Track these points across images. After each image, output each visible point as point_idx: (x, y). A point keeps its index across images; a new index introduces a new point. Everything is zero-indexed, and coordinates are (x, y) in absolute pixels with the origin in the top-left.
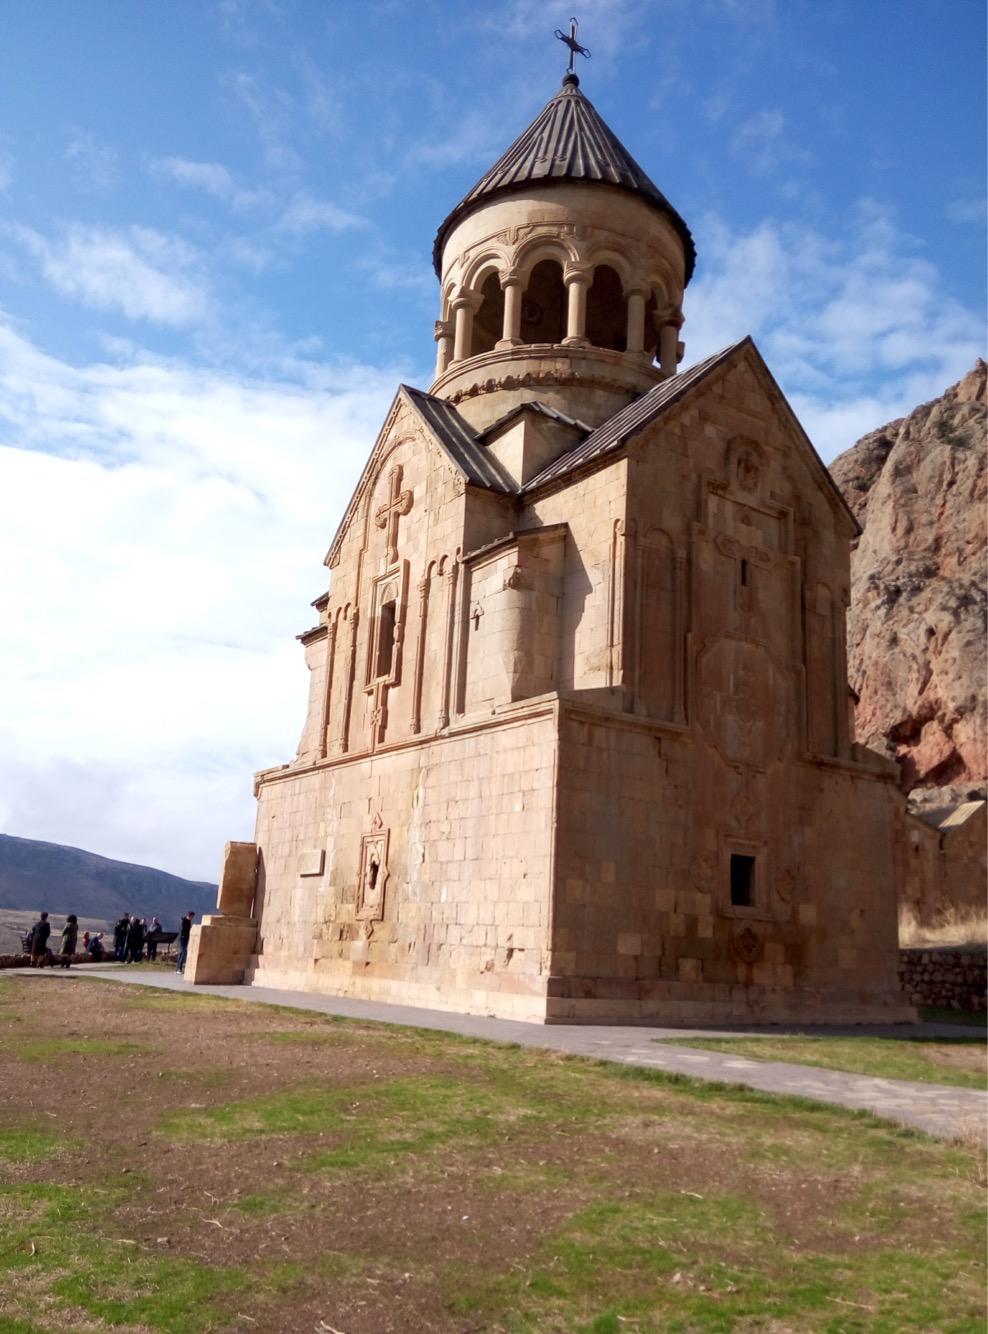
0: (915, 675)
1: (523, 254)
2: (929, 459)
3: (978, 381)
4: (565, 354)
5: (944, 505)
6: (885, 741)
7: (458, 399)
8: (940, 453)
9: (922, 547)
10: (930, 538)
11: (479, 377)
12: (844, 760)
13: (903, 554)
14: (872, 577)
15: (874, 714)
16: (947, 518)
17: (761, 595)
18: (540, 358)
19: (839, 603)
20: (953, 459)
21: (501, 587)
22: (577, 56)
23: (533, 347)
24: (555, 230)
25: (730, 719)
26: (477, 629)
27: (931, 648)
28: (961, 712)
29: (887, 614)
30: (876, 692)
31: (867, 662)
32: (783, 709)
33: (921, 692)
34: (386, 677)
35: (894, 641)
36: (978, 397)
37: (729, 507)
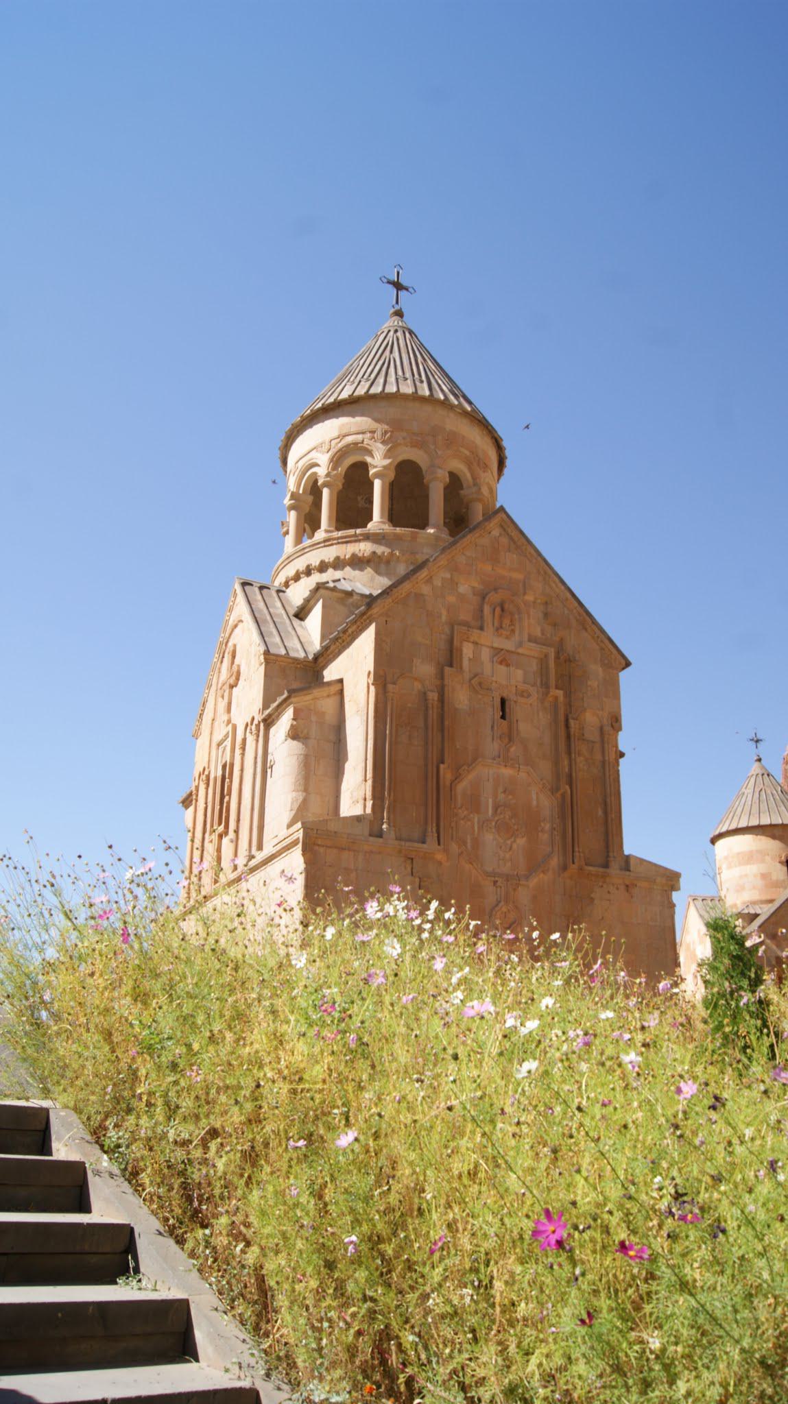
1: (336, 461)
7: (287, 585)
11: (300, 564)
12: (614, 870)
18: (347, 542)
19: (607, 729)
22: (402, 294)
23: (340, 534)
24: (360, 437)
25: (489, 838)
32: (547, 826)
37: (485, 654)
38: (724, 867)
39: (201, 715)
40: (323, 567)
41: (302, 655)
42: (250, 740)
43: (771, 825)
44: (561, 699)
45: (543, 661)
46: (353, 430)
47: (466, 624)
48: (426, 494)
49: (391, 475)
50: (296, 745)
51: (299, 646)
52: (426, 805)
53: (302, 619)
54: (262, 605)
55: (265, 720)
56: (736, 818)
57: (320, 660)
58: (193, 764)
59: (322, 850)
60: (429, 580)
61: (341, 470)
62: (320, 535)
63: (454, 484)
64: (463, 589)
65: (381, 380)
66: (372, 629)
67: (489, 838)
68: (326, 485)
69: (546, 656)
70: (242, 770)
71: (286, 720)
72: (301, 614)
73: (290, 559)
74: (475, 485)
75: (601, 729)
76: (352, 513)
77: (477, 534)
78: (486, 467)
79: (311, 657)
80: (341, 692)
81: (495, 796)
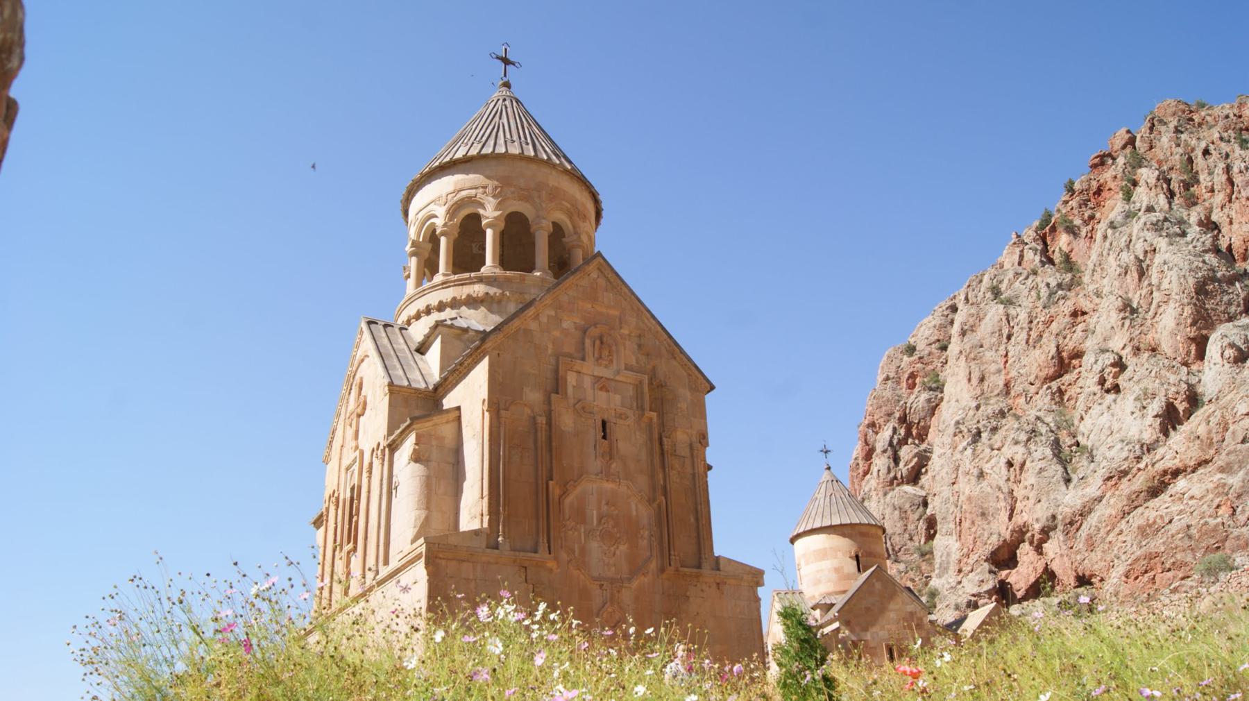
0: (1002, 504)
1: (453, 211)
2: (988, 318)
3: (1017, 250)
4: (480, 280)
5: (1006, 355)
6: (986, 565)
8: (995, 312)
9: (996, 392)
10: (1001, 383)
11: (420, 304)
12: (706, 570)
13: (981, 400)
14: (958, 423)
15: (975, 543)
17: (621, 445)
23: (456, 277)
24: (473, 192)
25: (595, 546)
27: (1012, 478)
28: (1046, 532)
29: (973, 454)
30: (973, 523)
31: (962, 498)
32: (646, 533)
33: (1010, 519)
35: (981, 475)
36: (1020, 264)
37: (587, 381)
38: (803, 563)
39: (331, 442)
40: (441, 307)
41: (423, 386)
42: (376, 463)
43: (841, 525)
44: (655, 420)
45: (638, 386)
46: (467, 185)
47: (569, 355)
48: (531, 242)
49: (502, 225)
50: (418, 468)
51: (420, 378)
52: (538, 519)
53: (423, 354)
54: (386, 341)
55: (389, 446)
56: (811, 521)
57: (440, 389)
58: (324, 487)
59: (443, 562)
60: (536, 317)
61: (457, 220)
62: (438, 278)
63: (557, 232)
64: (565, 325)
65: (491, 142)
66: (486, 361)
67: (595, 546)
68: (443, 234)
69: (641, 382)
70: (369, 492)
71: (409, 444)
72: (422, 349)
73: (411, 300)
74: (576, 233)
75: (691, 446)
76: (467, 258)
77: (578, 275)
78: (585, 218)
79: (431, 387)
80: (459, 418)
81: (599, 508)
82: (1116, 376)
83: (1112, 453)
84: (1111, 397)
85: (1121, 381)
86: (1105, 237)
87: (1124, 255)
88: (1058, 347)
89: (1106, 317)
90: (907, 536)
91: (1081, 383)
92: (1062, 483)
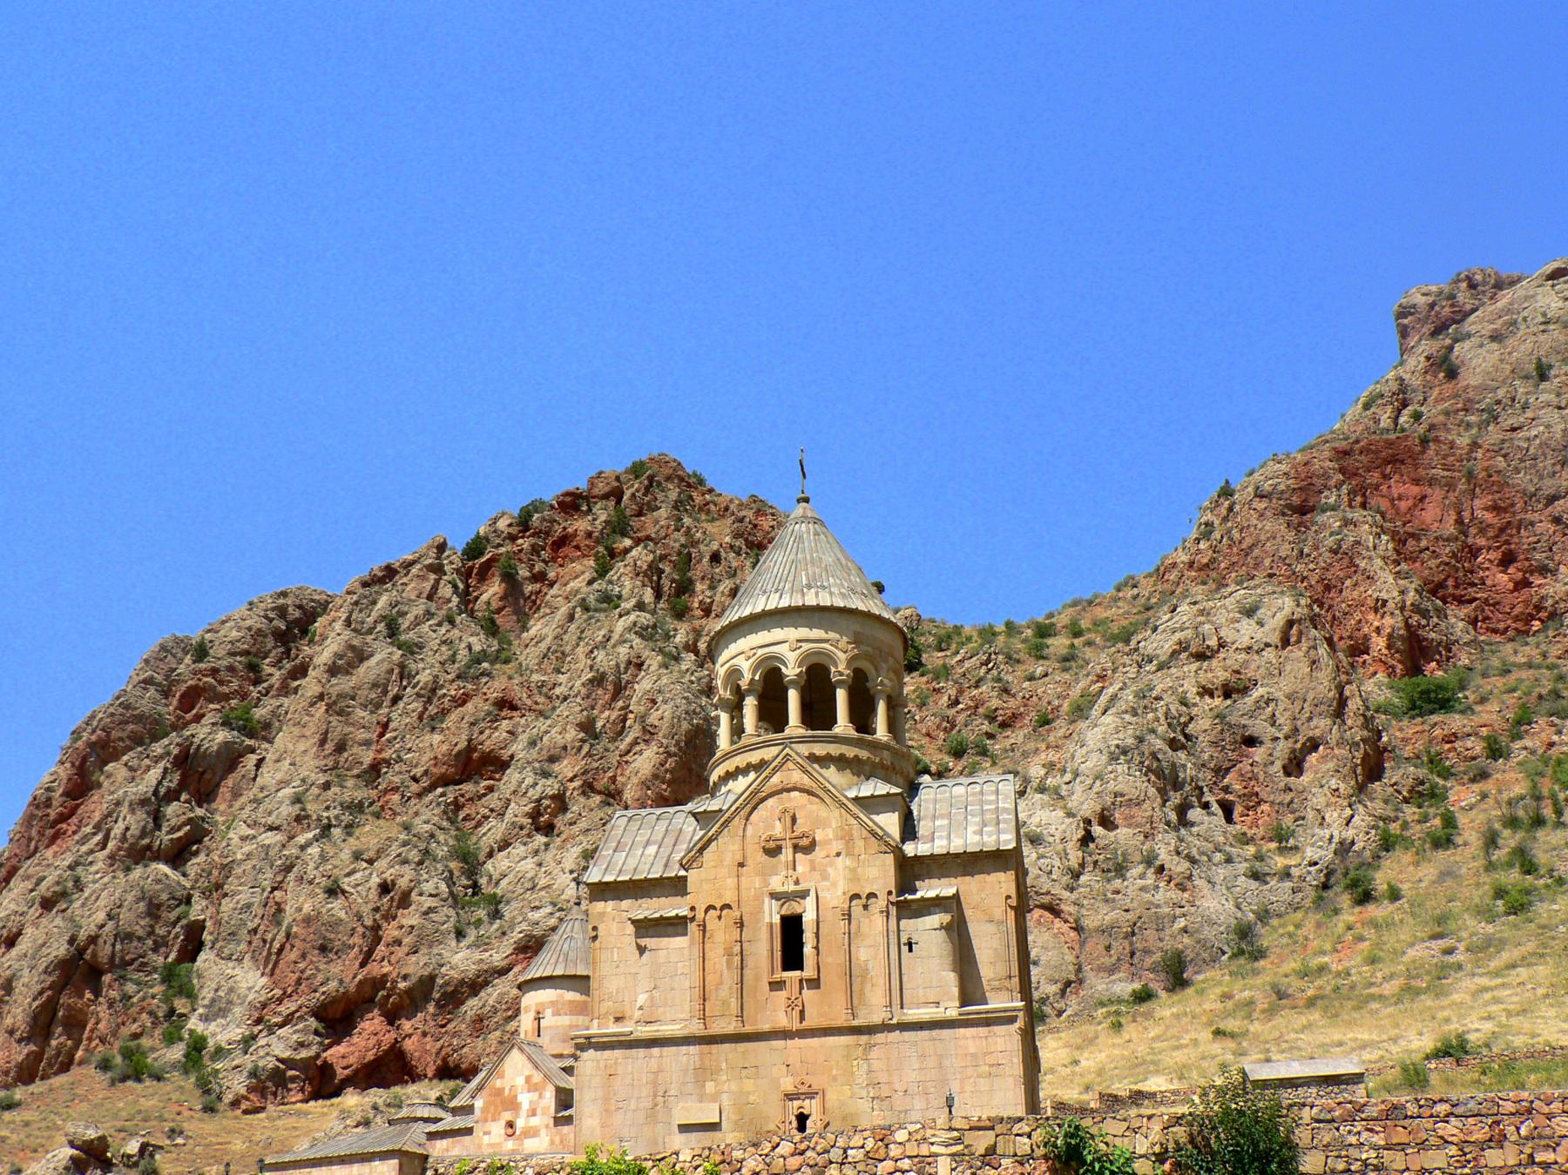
0: (356, 940)
2: (373, 661)
6: (312, 1022)
8: (383, 655)
9: (355, 772)
10: (368, 757)
14: (297, 800)
16: (389, 741)
20: (402, 666)
21: (937, 926)
26: (910, 950)
30: (304, 956)
33: (362, 965)
34: (798, 973)
36: (430, 598)
82: (554, 815)
83: (537, 915)
84: (540, 839)
85: (559, 822)
86: (571, 618)
87: (600, 656)
88: (470, 741)
89: (561, 730)
90: (150, 942)
91: (493, 800)
92: (453, 935)
